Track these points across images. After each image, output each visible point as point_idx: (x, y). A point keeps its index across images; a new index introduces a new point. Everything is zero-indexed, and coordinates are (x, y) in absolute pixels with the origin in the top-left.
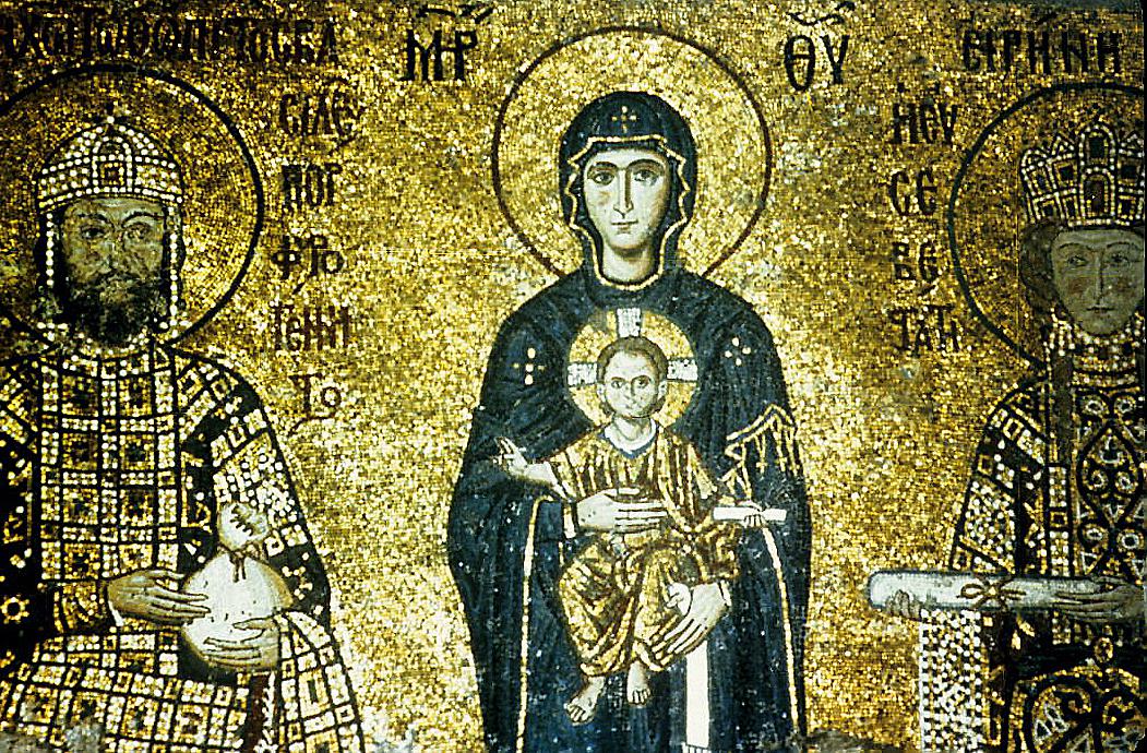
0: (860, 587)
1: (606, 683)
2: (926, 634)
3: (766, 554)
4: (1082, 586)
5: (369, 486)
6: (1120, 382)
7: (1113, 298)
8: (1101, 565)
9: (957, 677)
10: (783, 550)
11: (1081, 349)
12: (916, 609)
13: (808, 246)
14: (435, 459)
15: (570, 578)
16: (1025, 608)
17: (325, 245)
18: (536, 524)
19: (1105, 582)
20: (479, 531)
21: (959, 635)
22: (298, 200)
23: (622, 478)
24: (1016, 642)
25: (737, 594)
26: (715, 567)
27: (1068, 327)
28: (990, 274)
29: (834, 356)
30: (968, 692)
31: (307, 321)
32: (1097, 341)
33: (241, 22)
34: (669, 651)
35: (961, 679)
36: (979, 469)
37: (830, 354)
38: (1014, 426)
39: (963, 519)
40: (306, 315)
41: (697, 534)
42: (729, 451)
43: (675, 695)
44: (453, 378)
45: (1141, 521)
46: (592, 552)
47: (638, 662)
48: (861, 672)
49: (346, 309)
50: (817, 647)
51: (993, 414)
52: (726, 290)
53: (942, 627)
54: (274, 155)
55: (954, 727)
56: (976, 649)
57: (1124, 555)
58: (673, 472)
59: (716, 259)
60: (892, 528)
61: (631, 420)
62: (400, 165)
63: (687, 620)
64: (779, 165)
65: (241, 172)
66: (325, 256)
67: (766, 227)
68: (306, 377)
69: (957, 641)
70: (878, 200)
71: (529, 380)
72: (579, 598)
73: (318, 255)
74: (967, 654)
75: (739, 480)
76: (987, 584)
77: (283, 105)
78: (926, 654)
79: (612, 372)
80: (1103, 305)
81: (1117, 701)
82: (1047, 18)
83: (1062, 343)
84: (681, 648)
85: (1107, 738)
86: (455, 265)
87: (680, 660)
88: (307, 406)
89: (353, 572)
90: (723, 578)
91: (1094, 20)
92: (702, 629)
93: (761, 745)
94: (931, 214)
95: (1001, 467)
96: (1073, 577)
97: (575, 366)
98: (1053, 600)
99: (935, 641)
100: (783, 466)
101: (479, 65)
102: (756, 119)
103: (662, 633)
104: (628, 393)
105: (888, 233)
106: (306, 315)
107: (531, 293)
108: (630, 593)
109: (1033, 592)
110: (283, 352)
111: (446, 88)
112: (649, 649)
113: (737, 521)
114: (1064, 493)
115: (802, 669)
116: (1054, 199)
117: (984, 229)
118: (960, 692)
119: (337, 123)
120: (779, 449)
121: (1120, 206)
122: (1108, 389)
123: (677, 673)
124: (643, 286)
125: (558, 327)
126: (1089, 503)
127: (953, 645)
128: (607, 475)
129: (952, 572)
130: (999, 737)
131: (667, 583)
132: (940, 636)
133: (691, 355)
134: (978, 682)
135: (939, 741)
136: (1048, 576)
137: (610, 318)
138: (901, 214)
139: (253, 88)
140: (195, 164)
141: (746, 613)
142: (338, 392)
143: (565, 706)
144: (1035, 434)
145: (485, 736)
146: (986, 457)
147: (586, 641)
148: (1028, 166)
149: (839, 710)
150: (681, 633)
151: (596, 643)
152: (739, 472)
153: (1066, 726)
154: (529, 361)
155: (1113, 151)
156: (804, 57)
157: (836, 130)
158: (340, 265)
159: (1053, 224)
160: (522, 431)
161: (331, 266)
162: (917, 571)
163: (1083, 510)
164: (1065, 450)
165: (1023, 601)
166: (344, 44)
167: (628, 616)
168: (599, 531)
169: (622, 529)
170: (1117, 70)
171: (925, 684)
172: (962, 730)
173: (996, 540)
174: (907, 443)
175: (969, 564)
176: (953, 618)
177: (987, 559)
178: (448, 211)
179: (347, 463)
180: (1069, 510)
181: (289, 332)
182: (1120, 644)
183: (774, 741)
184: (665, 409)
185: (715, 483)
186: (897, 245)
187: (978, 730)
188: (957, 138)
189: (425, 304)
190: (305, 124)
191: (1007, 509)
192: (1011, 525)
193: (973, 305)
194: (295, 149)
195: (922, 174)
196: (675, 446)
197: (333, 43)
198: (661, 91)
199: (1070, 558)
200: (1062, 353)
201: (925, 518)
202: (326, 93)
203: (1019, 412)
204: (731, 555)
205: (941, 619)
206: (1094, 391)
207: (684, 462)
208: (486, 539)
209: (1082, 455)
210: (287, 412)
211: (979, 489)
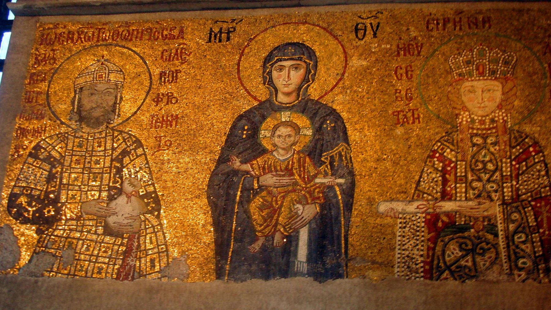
0: (374, 206)
1: (265, 239)
2: (401, 223)
3: (336, 195)
4: (470, 203)
5: (179, 172)
6: (489, 132)
7: (486, 103)
8: (479, 196)
9: (414, 237)
10: (343, 192)
11: (473, 121)
12: (397, 215)
13: (360, 90)
14: (205, 163)
15: (254, 203)
16: (445, 212)
17: (173, 95)
18: (242, 184)
19: (479, 202)
20: (219, 187)
21: (415, 222)
22: (165, 82)
23: (278, 168)
24: (440, 224)
25: (322, 207)
26: (314, 199)
27: (467, 113)
28: (435, 97)
29: (369, 126)
30: (418, 242)
31: (163, 119)
32: (480, 118)
33: (151, 29)
34: (294, 226)
35: (415, 238)
36: (428, 163)
37: (367, 126)
38: (442, 149)
39: (419, 181)
40: (163, 117)
41: (308, 188)
42: (323, 159)
43: (294, 243)
44: (215, 136)
45: (497, 180)
46: (264, 193)
47: (279, 232)
48: (372, 236)
49: (178, 115)
50: (354, 227)
51: (434, 144)
52: (326, 105)
53: (408, 220)
54: (157, 68)
55: (410, 255)
56: (423, 227)
57: (490, 192)
58: (300, 167)
59: (323, 94)
60: (389, 186)
61: (283, 149)
62: (203, 69)
63: (301, 217)
64: (351, 64)
65: (145, 74)
66: (172, 99)
67: (343, 84)
68: (160, 137)
69: (414, 225)
70: (390, 75)
71: (244, 136)
72: (257, 209)
73: (169, 98)
74: (418, 229)
75: (326, 169)
76: (429, 203)
77: (162, 53)
78: (400, 230)
79: (278, 133)
80: (482, 105)
81: (483, 245)
82: (461, 13)
83: (464, 119)
84: (298, 226)
85: (478, 259)
86: (220, 100)
87: (297, 231)
88: (159, 146)
89: (170, 200)
90: (317, 203)
91: (480, 12)
92: (307, 220)
93: (328, 261)
94: (411, 79)
95: (437, 162)
96: (467, 199)
97: (263, 131)
98: (458, 208)
99: (404, 225)
100: (345, 164)
101: (236, 37)
102: (342, 50)
103: (290, 221)
104: (283, 140)
105: (393, 86)
106: (163, 117)
107: (248, 108)
108: (278, 207)
109: (448, 206)
110: (153, 129)
111: (223, 45)
112: (284, 227)
113: (324, 183)
114: (463, 170)
115: (347, 235)
116: (462, 71)
117: (434, 82)
118: (414, 243)
119: (181, 57)
120: (344, 158)
121: (491, 72)
122: (484, 134)
123: (295, 236)
124: (292, 105)
125: (258, 118)
126: (475, 174)
127: (412, 226)
128: (273, 167)
129: (413, 200)
130: (430, 258)
131: (294, 205)
132: (407, 223)
133: (310, 126)
134: (423, 239)
135: (403, 261)
136: (455, 200)
137: (278, 115)
138: (399, 80)
139: (153, 48)
140: (130, 72)
141: (326, 215)
142: (171, 142)
143: (249, 247)
144: (452, 150)
145: (216, 257)
146: (431, 159)
147: (259, 224)
148: (452, 61)
149: (361, 249)
150: (298, 222)
151: (261, 225)
152: (327, 166)
153: (460, 254)
154: (245, 130)
155: (488, 54)
156: (363, 30)
157: (374, 52)
158: (177, 101)
159: (461, 79)
160: (240, 154)
161: (173, 102)
162: (398, 201)
163: (472, 176)
164: (463, 156)
165: (444, 209)
166: (187, 33)
167: (276, 215)
168: (266, 186)
169: (276, 186)
170: (490, 27)
171: (399, 241)
172: (414, 256)
173: (433, 188)
174: (397, 156)
175: (421, 196)
176: (413, 217)
177: (429, 195)
178: (219, 83)
179: (172, 165)
180: (466, 176)
181: (156, 122)
182: (486, 223)
183: (333, 260)
184: (298, 144)
185: (316, 169)
186: (396, 90)
187: (421, 256)
188: (422, 53)
189: (207, 113)
190: (170, 58)
191: (439, 177)
192: (440, 182)
193: (428, 108)
194: (165, 66)
195: (407, 66)
196: (301, 157)
197: (183, 32)
198: (304, 42)
199: (466, 192)
200: (464, 123)
201: (403, 182)
202: (178, 49)
203: (445, 143)
204: (321, 195)
205: (408, 217)
206: (476, 135)
207: (305, 162)
208: (222, 189)
209: (473, 157)
210: (152, 148)
211: (427, 170)
